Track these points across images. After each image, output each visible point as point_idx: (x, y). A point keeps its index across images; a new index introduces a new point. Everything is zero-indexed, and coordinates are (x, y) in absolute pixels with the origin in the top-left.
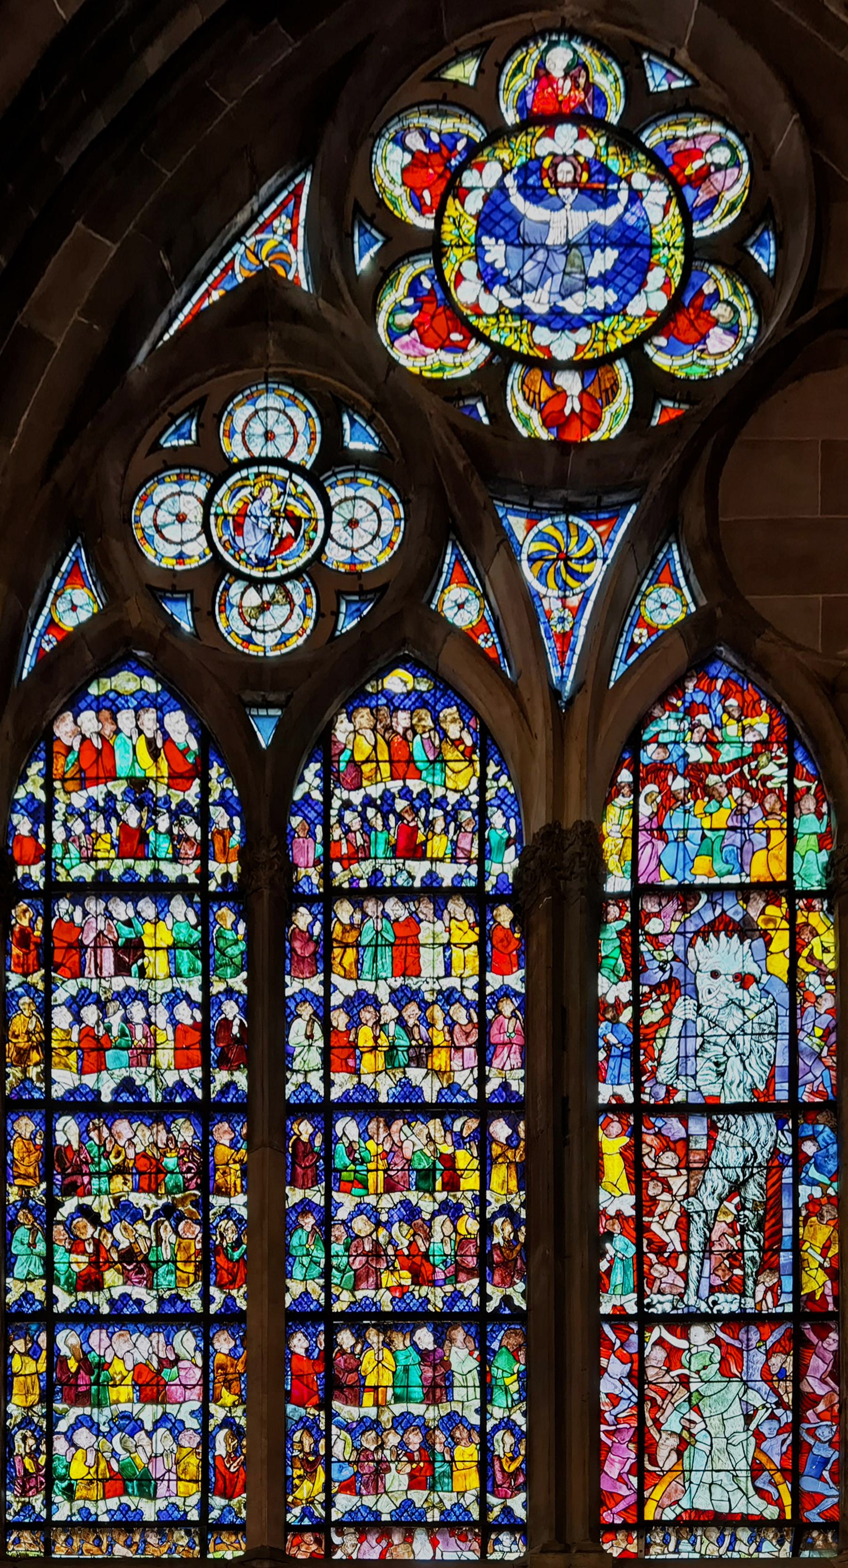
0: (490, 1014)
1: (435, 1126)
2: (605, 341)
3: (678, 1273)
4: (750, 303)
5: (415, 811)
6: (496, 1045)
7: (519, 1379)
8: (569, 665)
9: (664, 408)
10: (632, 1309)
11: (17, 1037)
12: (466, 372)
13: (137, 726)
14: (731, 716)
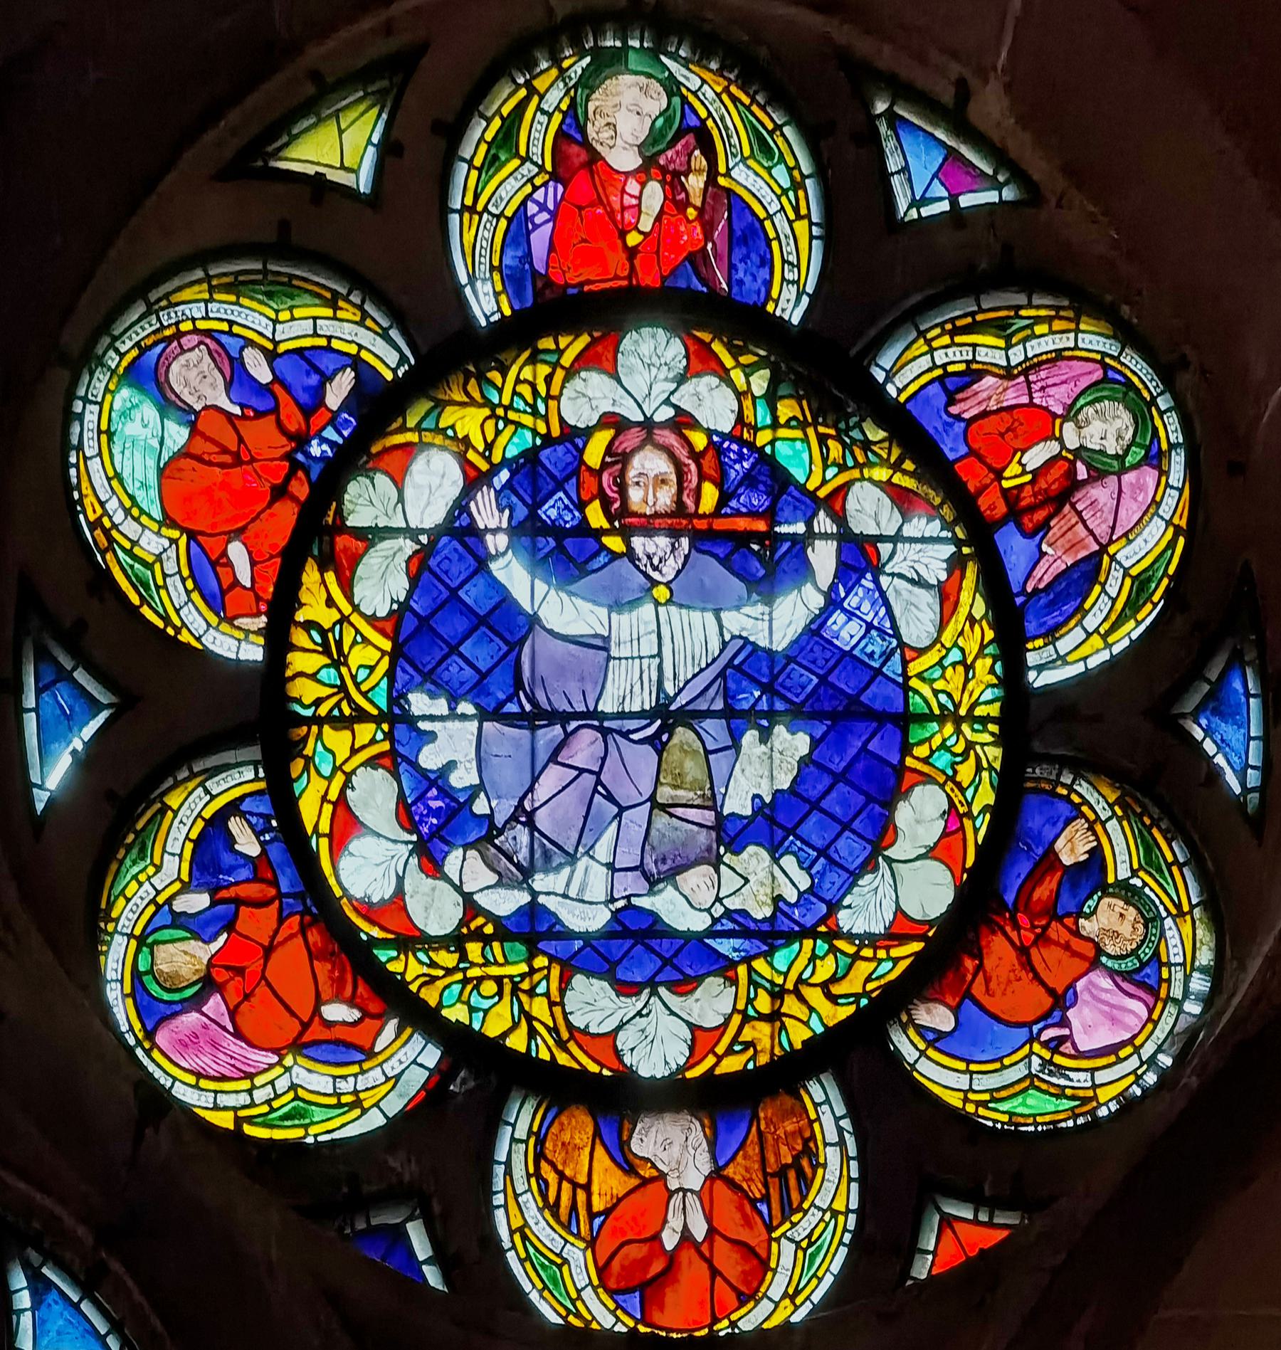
2: (775, 1017)
4: (1190, 890)
9: (947, 1222)
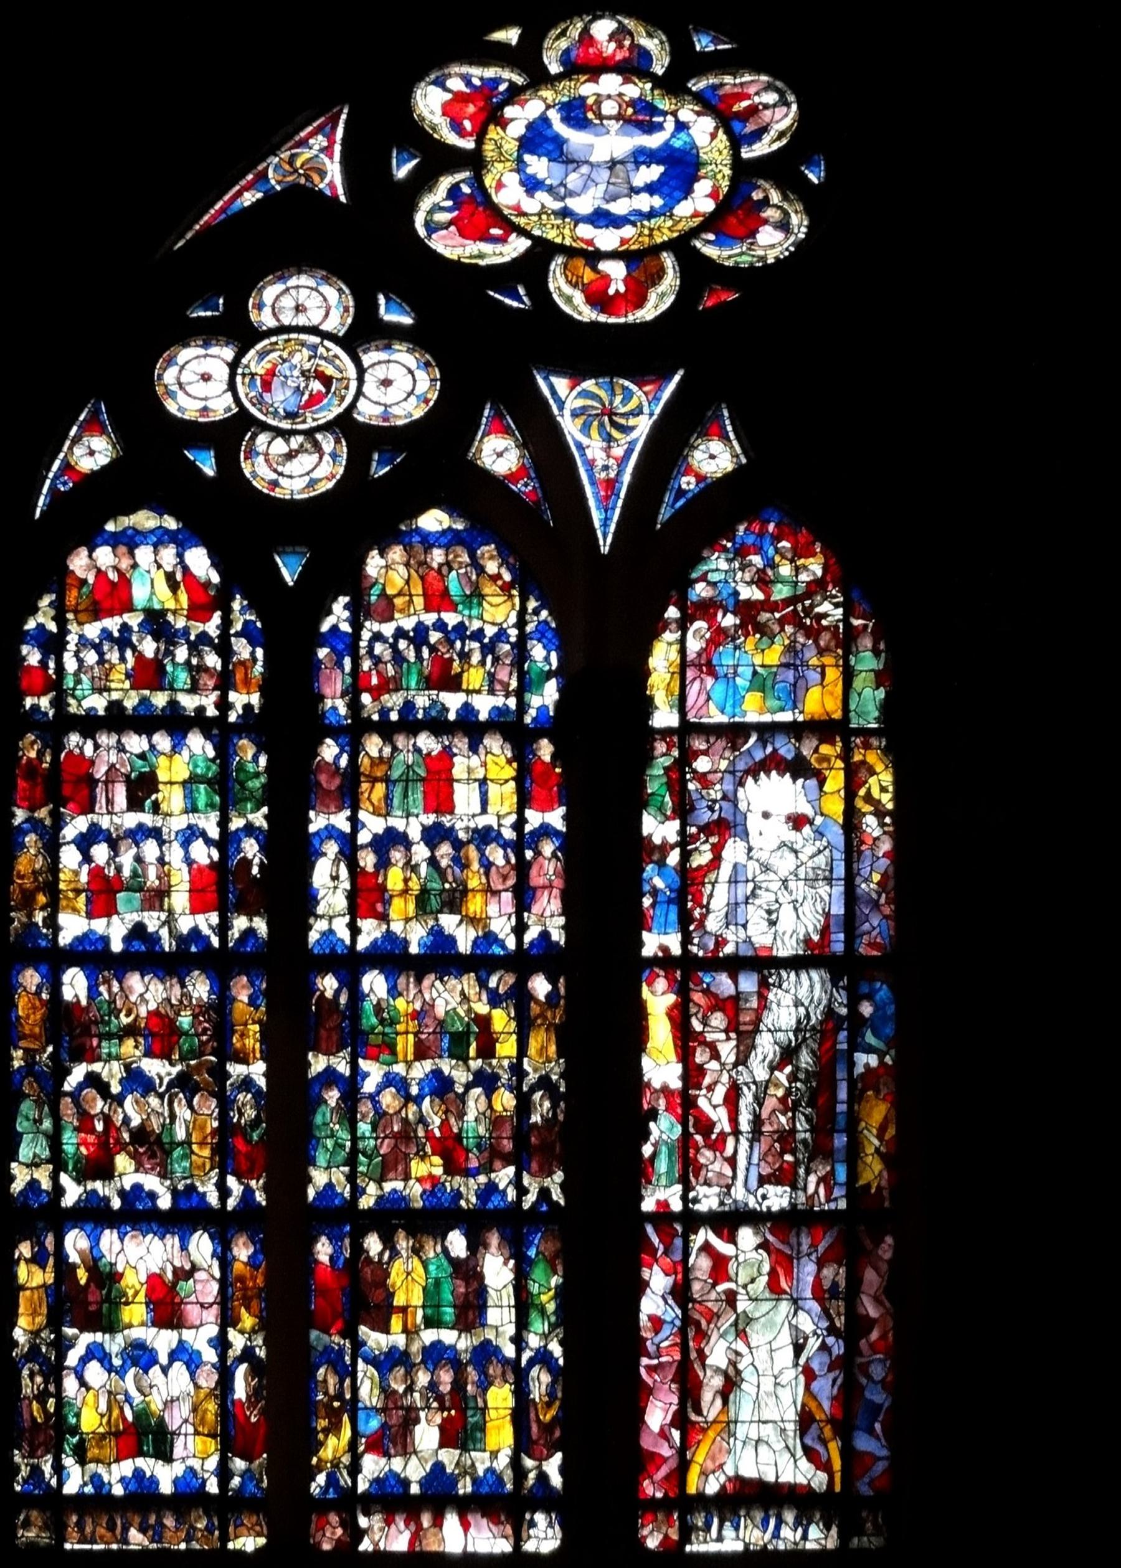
0: (529, 854)
1: (469, 983)
3: (726, 1159)
5: (451, 644)
6: (535, 889)
7: (556, 1297)
8: (613, 509)
10: (676, 1206)
11: (22, 877)
12: (507, 259)
13: (156, 561)
14: (783, 557)
